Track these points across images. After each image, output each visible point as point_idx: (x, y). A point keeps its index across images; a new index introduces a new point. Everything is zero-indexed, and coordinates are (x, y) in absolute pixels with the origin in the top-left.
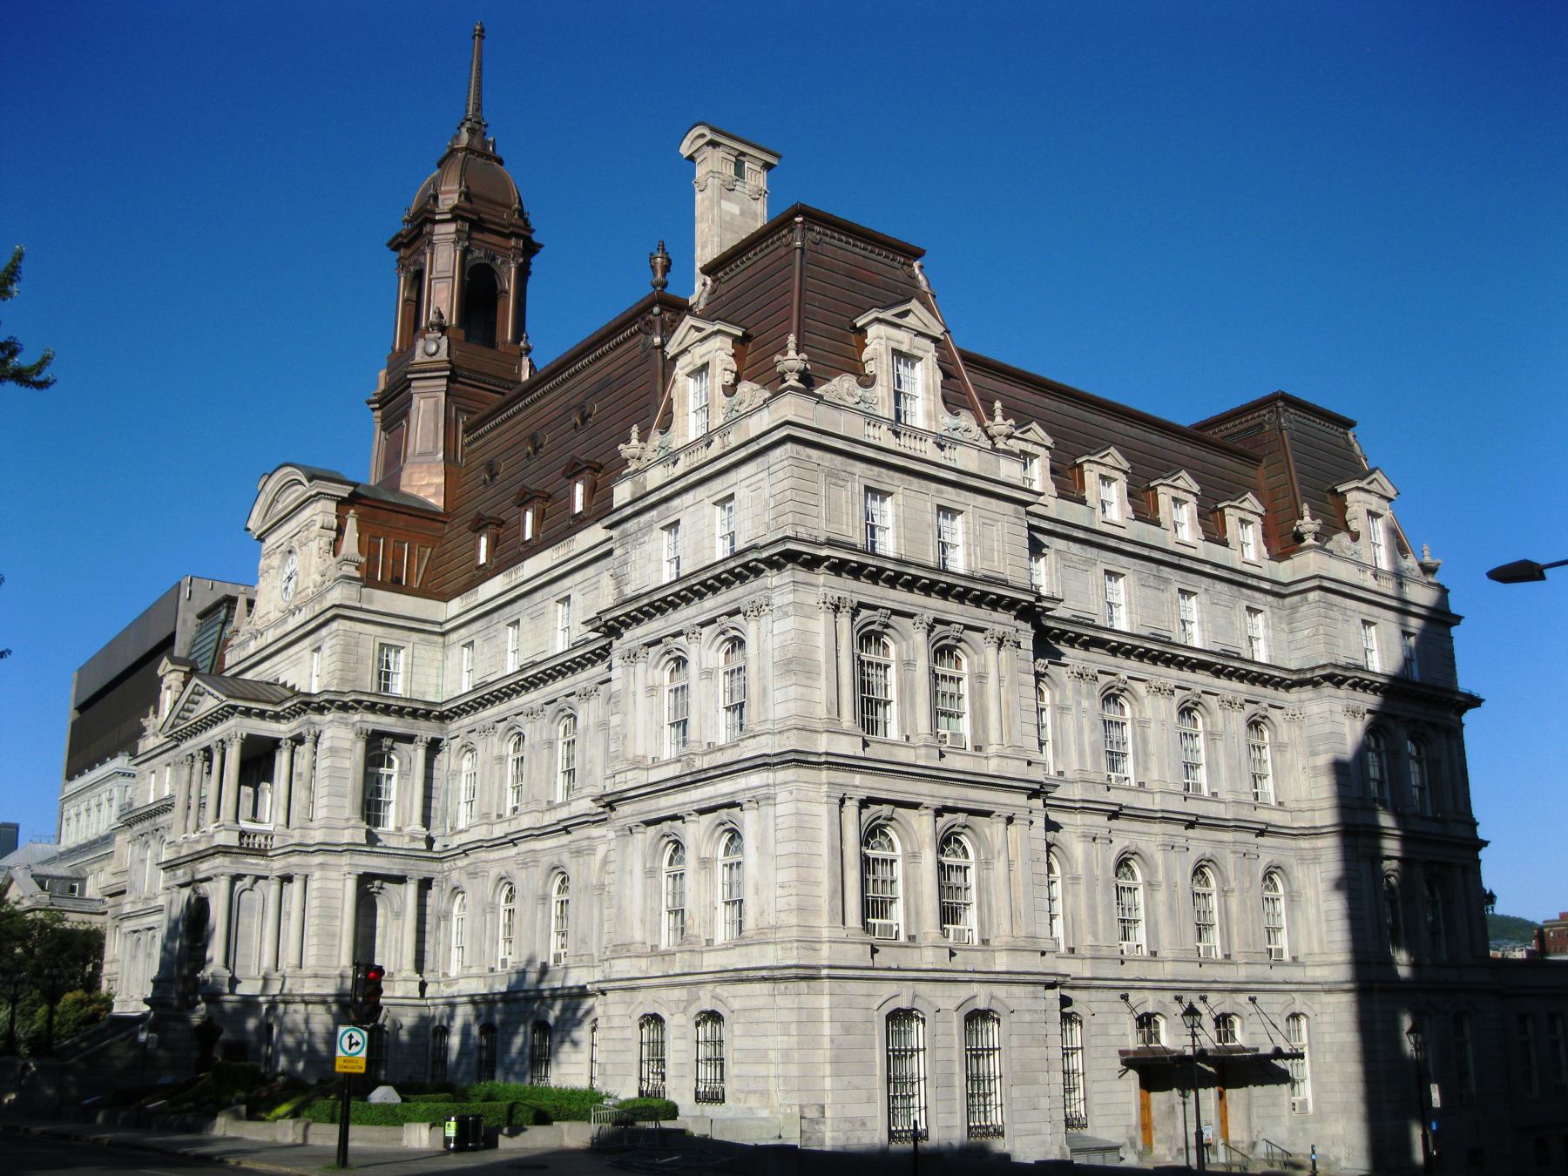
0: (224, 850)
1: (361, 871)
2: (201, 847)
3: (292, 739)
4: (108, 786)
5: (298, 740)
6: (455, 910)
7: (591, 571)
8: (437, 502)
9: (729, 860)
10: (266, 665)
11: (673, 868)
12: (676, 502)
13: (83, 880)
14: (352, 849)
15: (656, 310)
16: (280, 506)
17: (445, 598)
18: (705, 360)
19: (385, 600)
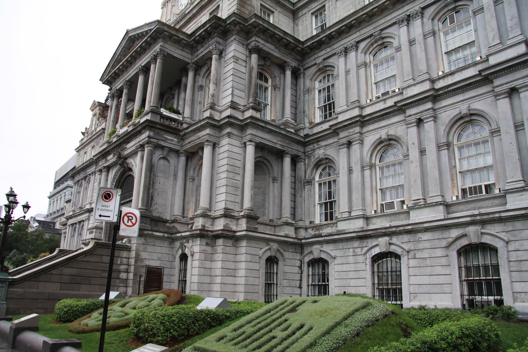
1: (258, 140)
4: (64, 191)
6: (317, 178)
13: (54, 224)
14: (254, 123)
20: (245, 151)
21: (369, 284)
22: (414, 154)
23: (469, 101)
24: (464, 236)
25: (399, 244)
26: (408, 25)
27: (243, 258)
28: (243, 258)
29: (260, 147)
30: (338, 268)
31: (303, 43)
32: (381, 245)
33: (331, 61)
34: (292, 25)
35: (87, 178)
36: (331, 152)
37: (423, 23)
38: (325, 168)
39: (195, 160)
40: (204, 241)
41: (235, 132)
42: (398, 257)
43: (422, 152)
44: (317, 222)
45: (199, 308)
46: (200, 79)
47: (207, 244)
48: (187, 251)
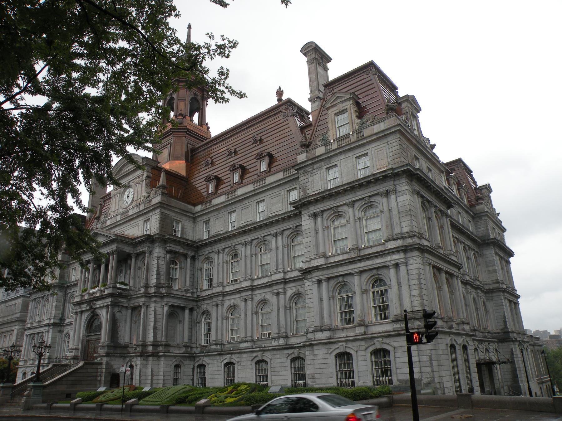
0: (111, 295)
1: (170, 304)
2: (98, 295)
3: (136, 254)
5: (138, 255)
6: (203, 320)
7: (276, 190)
8: (183, 173)
9: (375, 289)
10: (117, 228)
11: (340, 295)
12: (336, 159)
16: (123, 171)
17: (195, 205)
18: (345, 108)
19: (174, 202)
21: (223, 377)
22: (243, 316)
24: (257, 356)
25: (235, 358)
26: (246, 247)
27: (162, 366)
28: (162, 366)
30: (210, 369)
31: (197, 243)
32: (227, 359)
33: (212, 255)
34: (193, 226)
35: (45, 298)
36: (209, 308)
37: (251, 248)
38: (207, 316)
39: (136, 312)
40: (142, 358)
41: (158, 299)
42: (234, 364)
43: (246, 315)
44: (203, 344)
45: (143, 390)
46: (139, 263)
48: (133, 363)
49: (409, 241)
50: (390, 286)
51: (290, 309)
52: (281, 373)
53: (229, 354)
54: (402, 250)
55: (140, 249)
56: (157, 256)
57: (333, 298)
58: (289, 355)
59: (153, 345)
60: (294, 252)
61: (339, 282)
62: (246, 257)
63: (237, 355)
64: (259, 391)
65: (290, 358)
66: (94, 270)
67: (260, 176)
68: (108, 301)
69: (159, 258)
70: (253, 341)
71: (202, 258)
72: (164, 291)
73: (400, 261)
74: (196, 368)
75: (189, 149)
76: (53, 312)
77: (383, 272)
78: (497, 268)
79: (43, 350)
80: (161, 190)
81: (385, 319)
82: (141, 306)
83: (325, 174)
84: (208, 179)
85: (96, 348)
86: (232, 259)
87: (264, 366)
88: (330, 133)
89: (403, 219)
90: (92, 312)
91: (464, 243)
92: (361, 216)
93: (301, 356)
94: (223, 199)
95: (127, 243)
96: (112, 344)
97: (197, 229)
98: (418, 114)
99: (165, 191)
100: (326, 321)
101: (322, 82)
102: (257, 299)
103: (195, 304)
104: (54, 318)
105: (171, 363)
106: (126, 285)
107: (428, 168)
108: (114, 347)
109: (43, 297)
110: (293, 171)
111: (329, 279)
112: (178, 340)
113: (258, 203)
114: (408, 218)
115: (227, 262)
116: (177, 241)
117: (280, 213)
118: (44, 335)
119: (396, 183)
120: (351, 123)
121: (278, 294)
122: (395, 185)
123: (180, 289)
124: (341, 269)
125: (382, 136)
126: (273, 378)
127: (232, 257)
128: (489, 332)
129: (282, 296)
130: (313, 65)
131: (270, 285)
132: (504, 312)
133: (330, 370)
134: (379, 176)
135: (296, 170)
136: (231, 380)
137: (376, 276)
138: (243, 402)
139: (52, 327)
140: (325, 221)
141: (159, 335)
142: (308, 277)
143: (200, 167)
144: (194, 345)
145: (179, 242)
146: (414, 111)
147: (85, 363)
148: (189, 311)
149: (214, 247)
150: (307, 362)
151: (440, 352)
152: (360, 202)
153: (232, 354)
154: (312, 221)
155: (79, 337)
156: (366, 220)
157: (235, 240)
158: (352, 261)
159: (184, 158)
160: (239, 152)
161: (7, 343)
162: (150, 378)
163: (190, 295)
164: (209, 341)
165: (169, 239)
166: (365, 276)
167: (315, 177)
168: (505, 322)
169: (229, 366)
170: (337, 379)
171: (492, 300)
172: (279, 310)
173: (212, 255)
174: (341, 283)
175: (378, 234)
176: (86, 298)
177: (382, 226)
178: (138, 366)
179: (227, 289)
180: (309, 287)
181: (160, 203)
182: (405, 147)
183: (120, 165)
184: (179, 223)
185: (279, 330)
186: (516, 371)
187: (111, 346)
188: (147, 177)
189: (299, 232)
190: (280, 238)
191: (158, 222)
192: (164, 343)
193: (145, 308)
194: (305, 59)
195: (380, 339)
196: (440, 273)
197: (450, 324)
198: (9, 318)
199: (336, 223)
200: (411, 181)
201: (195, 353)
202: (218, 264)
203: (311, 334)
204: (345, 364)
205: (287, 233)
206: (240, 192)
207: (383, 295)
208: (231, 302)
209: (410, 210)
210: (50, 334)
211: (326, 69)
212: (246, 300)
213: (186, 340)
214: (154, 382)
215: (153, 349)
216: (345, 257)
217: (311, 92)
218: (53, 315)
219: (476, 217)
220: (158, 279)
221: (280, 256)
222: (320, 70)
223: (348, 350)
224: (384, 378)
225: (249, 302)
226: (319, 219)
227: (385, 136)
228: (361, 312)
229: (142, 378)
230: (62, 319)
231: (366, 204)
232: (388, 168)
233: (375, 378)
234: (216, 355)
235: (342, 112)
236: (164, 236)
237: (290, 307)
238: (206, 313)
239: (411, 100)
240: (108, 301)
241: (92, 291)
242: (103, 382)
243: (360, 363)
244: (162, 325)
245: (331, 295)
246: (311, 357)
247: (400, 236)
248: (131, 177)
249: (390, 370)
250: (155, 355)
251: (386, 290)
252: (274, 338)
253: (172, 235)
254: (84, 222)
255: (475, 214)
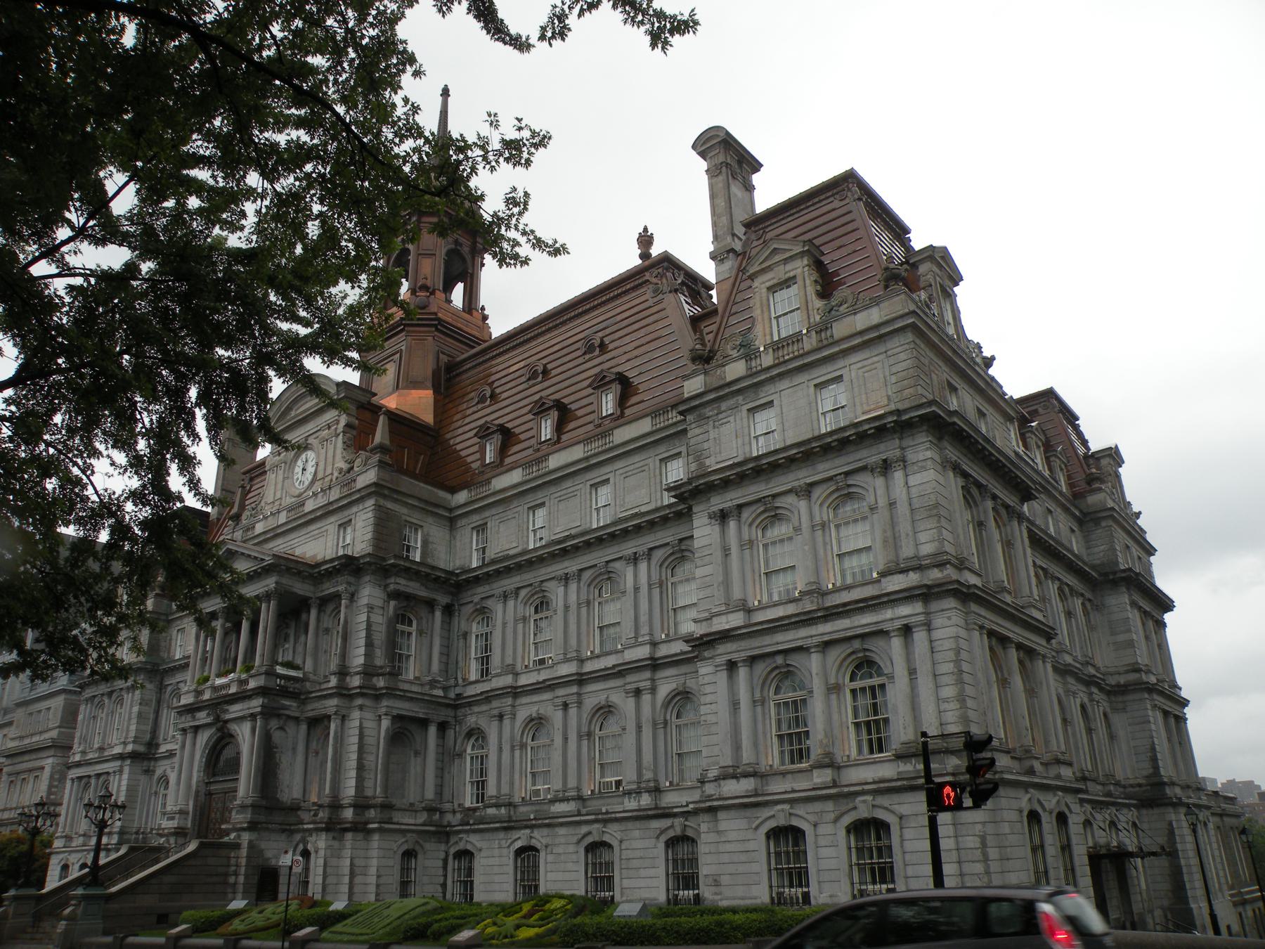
0: (261, 691)
1: (395, 712)
2: (233, 690)
5: (324, 602)
6: (469, 750)
7: (636, 458)
8: (428, 418)
9: (858, 684)
10: (279, 541)
11: (779, 697)
12: (770, 389)
15: (666, 264)
16: (293, 413)
17: (453, 490)
18: (791, 274)
19: (407, 484)
20: (380, 725)
21: (511, 879)
22: (558, 740)
23: (609, 692)
24: (590, 833)
25: (539, 838)
26: (566, 586)
27: (375, 853)
28: (375, 853)
29: (398, 718)
30: (483, 861)
31: (457, 575)
32: (521, 838)
33: (489, 603)
34: (447, 537)
36: (483, 723)
40: (331, 835)
41: (367, 702)
43: (566, 739)
44: (468, 804)
45: (331, 909)
46: (326, 618)
47: (334, 838)
48: (310, 847)
49: (935, 575)
50: (891, 677)
51: (665, 727)
52: (643, 873)
53: (526, 827)
54: (919, 595)
55: (329, 588)
56: (367, 605)
57: (763, 702)
58: (663, 832)
59: (355, 806)
60: (674, 599)
61: (776, 668)
62: (567, 608)
63: (545, 831)
64: (593, 913)
65: (664, 838)
66: (226, 633)
67: (600, 425)
68: (256, 704)
69: (371, 608)
70: (580, 798)
71: (468, 609)
72: (381, 683)
73: (913, 619)
74: (451, 858)
75: (442, 364)
76: (133, 727)
77: (876, 645)
78: (1135, 637)
79: (108, 815)
80: (377, 457)
81: (881, 751)
82: (329, 717)
83: (745, 424)
84: (484, 433)
85: (226, 810)
86: (536, 612)
87: (606, 856)
88: (758, 330)
89: (921, 526)
90: (218, 730)
91: (1059, 579)
92: (825, 518)
93: (690, 833)
94: (515, 477)
95: (299, 573)
96: (264, 803)
97: (458, 544)
98: (956, 289)
99: (387, 459)
100: (747, 756)
101: (740, 216)
102: (590, 702)
103: (451, 712)
104: (134, 742)
105: (395, 846)
106: (297, 668)
107: (979, 409)
108: (266, 808)
109: (110, 694)
110: (674, 417)
111: (752, 660)
112: (412, 795)
113: (595, 486)
114: (932, 523)
115: (524, 619)
116: (412, 572)
117: (644, 509)
118: (111, 779)
119: (906, 443)
120: (804, 308)
121: (638, 692)
122: (903, 449)
123: (416, 678)
124: (780, 637)
125: (874, 338)
126: (626, 883)
127: (536, 608)
128: (1117, 784)
129: (646, 698)
130: (720, 178)
131: (620, 672)
132: (1152, 737)
133: (755, 867)
134: (866, 427)
135: (681, 413)
136: (530, 887)
137: (860, 655)
138: (556, 938)
139: (128, 762)
140: (745, 529)
141: (369, 784)
142: (706, 654)
143: (465, 406)
144: (447, 806)
145: (417, 573)
146: (947, 283)
147: (202, 845)
148: (438, 730)
149: (495, 585)
150: (702, 848)
151: (1006, 828)
152: (824, 486)
153: (532, 827)
154: (717, 528)
155: (189, 786)
156: (838, 526)
157: (543, 571)
158: (807, 620)
159: (430, 384)
160: (554, 373)
161: (28, 796)
162: (346, 880)
163: (440, 693)
164: (480, 797)
165: (393, 565)
166: (835, 654)
167: (723, 429)
168: (1154, 760)
169: (527, 853)
170: (771, 887)
171: (1124, 710)
172: (639, 728)
173: (489, 603)
174: (781, 669)
175: (864, 559)
176: (207, 696)
177: (873, 540)
178: (322, 853)
179: (524, 680)
180: (709, 677)
181: (375, 484)
182: (926, 362)
183: (288, 399)
184: (416, 530)
185: (640, 774)
186: (1181, 873)
187: (260, 807)
188: (348, 425)
189: (686, 554)
190: (643, 566)
191: (370, 528)
192: (379, 800)
193: (339, 722)
194: (703, 165)
195: (869, 798)
196: (1004, 648)
197: (1027, 763)
198: (35, 739)
199: (769, 533)
200: (940, 439)
201: (449, 825)
202: (504, 624)
203: (712, 785)
204: (787, 853)
205: (659, 555)
206: (555, 461)
207: (874, 697)
208: (533, 711)
209: (937, 505)
210: (125, 776)
211: (749, 188)
212: (565, 706)
213: (430, 794)
214: (356, 889)
215: (355, 814)
216: (791, 609)
217: (716, 237)
218: (132, 734)
219: (1087, 520)
220: (369, 655)
221: (644, 606)
222: (736, 190)
223: (795, 822)
224: (877, 887)
225: (573, 711)
226: (732, 524)
227: (881, 337)
228: (826, 736)
229: (330, 880)
230: (152, 744)
231: (837, 490)
232: (888, 409)
233: (857, 886)
234: (496, 829)
235: (787, 283)
236: (384, 559)
237: (666, 722)
238: (476, 734)
239: (940, 258)
240: (256, 704)
241: (219, 681)
242: (240, 888)
243: (824, 852)
244: (376, 759)
245: (758, 695)
246: (712, 837)
247: (915, 563)
248: (310, 427)
249: (892, 868)
250: (359, 828)
251: (882, 686)
252: (628, 793)
253: (401, 558)
254: (206, 527)
255: (1085, 514)
